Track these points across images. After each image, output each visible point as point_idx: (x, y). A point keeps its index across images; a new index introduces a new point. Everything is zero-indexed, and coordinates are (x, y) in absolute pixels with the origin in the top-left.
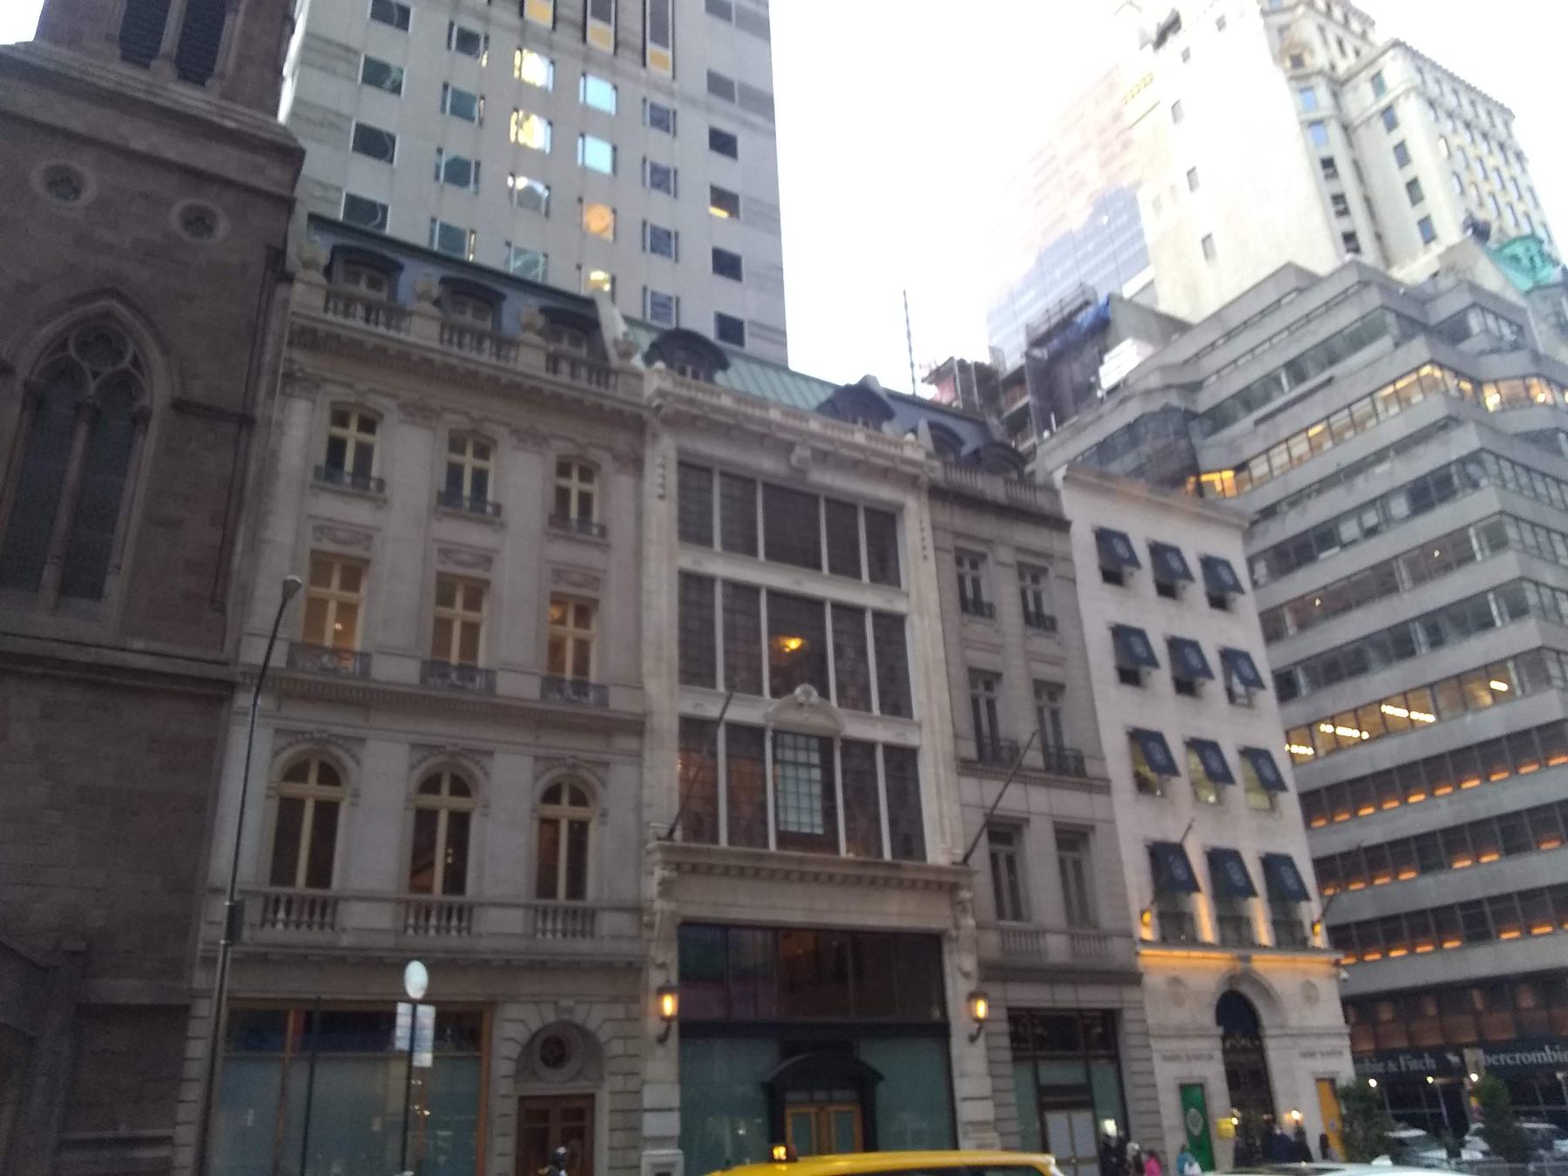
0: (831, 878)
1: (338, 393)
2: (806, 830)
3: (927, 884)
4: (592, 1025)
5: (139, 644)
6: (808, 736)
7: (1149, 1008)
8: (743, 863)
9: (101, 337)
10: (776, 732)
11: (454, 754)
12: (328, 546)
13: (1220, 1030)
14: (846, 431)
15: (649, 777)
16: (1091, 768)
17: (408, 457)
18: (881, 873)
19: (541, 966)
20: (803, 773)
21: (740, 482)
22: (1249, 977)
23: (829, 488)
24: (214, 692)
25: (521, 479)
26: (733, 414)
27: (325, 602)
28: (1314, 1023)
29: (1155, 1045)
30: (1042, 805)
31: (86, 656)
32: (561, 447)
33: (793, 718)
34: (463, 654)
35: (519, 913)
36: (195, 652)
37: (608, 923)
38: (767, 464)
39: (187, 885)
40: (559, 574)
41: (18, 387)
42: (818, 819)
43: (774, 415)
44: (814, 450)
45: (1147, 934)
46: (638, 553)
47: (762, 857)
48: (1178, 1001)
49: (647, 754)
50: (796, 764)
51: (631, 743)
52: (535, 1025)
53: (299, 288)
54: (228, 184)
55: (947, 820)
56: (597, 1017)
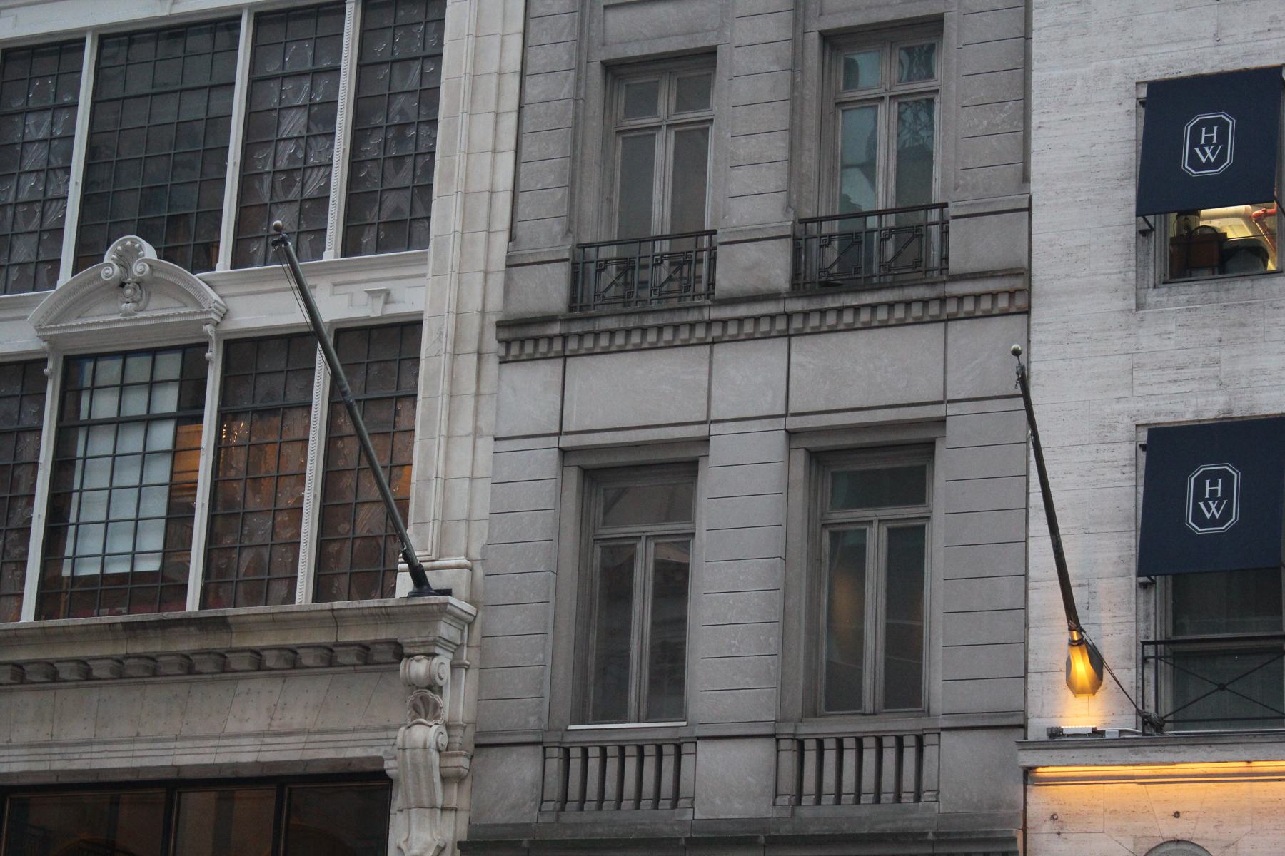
0: (85, 672)
6: (153, 352)
10: (72, 364)
18: (188, 644)
20: (132, 441)
33: (106, 319)
42: (153, 539)
45: (1081, 714)
50: (120, 423)
55: (476, 476)
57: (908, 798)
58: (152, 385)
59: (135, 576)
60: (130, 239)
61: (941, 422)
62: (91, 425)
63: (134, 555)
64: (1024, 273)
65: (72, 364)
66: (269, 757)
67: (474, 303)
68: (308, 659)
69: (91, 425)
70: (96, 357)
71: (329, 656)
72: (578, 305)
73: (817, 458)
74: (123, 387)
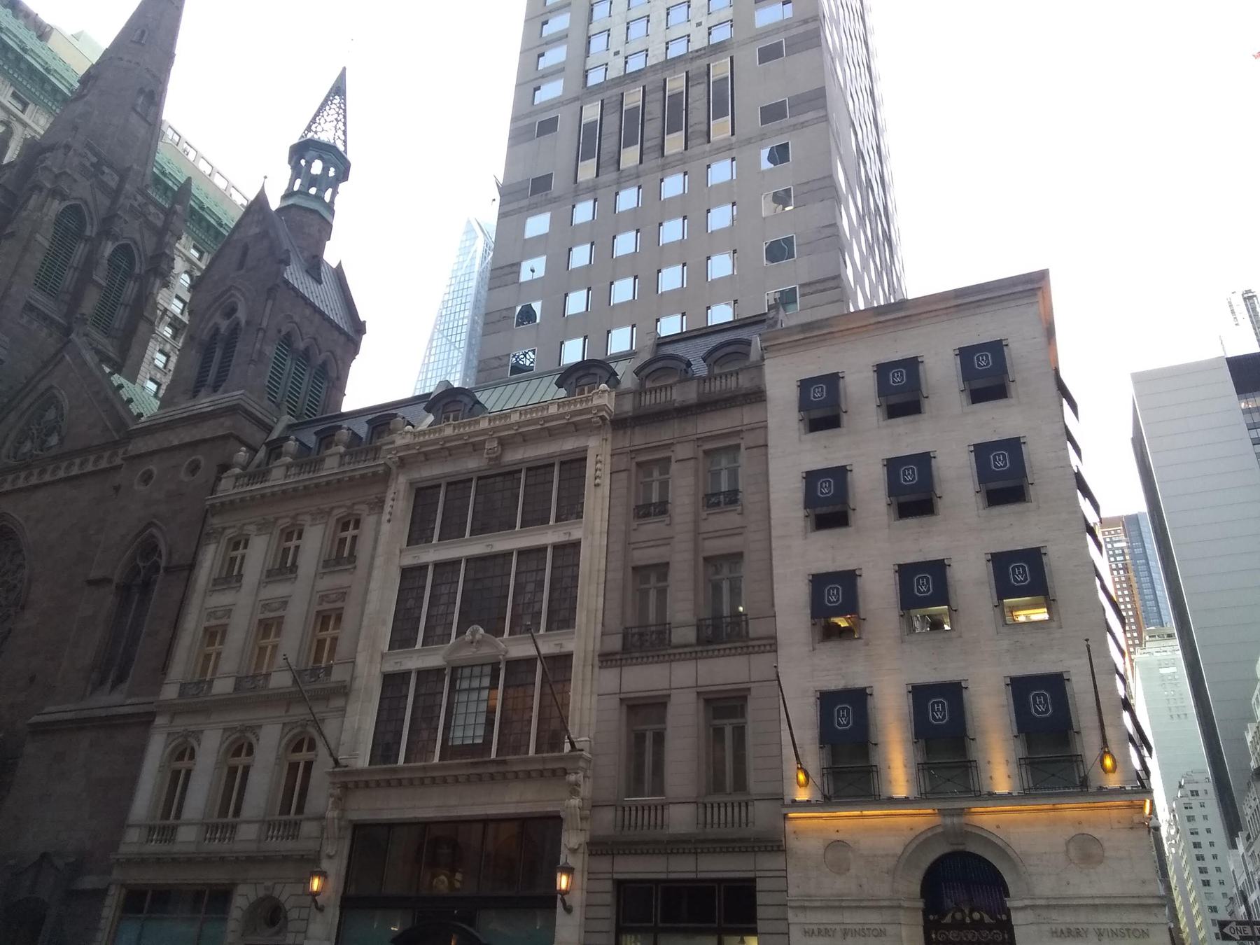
0: (456, 780)
1: (230, 533)
2: (466, 742)
3: (422, 779)
4: (283, 899)
5: (129, 702)
7: (793, 876)
8: (377, 777)
9: (149, 548)
10: (454, 670)
11: (241, 731)
12: (213, 622)
13: (920, 904)
14: (469, 424)
15: (347, 725)
16: (756, 629)
17: (258, 554)
18: (493, 769)
19: (265, 860)
20: (474, 696)
21: (458, 485)
22: (967, 833)
23: (522, 461)
24: (145, 721)
25: (314, 543)
26: (459, 437)
27: (210, 655)
28: (1086, 890)
29: (791, 916)
30: (680, 681)
31: (103, 713)
32: (339, 513)
33: (466, 654)
34: (328, 660)
35: (256, 826)
36: (142, 700)
37: (308, 828)
38: (472, 464)
39: (121, 824)
40: (323, 598)
41: (113, 587)
42: (480, 732)
43: (515, 418)
44: (499, 438)
45: (803, 795)
46: (371, 566)
47: (395, 771)
48: (840, 868)
49: (348, 709)
50: (470, 690)
51: (339, 702)
52: (253, 898)
53: (223, 481)
54: (205, 441)
55: (590, 707)
56: (286, 895)
57: (743, 825)
58: (481, 676)
59: (474, 745)
60: (475, 626)
61: (749, 689)
62: (460, 691)
63: (474, 737)
64: (774, 638)
65: (454, 670)
66: (520, 811)
67: (590, 648)
68: (533, 774)
69: (460, 691)
70: (462, 667)
71: (541, 773)
72: (625, 648)
73: (707, 701)
74: (471, 677)
